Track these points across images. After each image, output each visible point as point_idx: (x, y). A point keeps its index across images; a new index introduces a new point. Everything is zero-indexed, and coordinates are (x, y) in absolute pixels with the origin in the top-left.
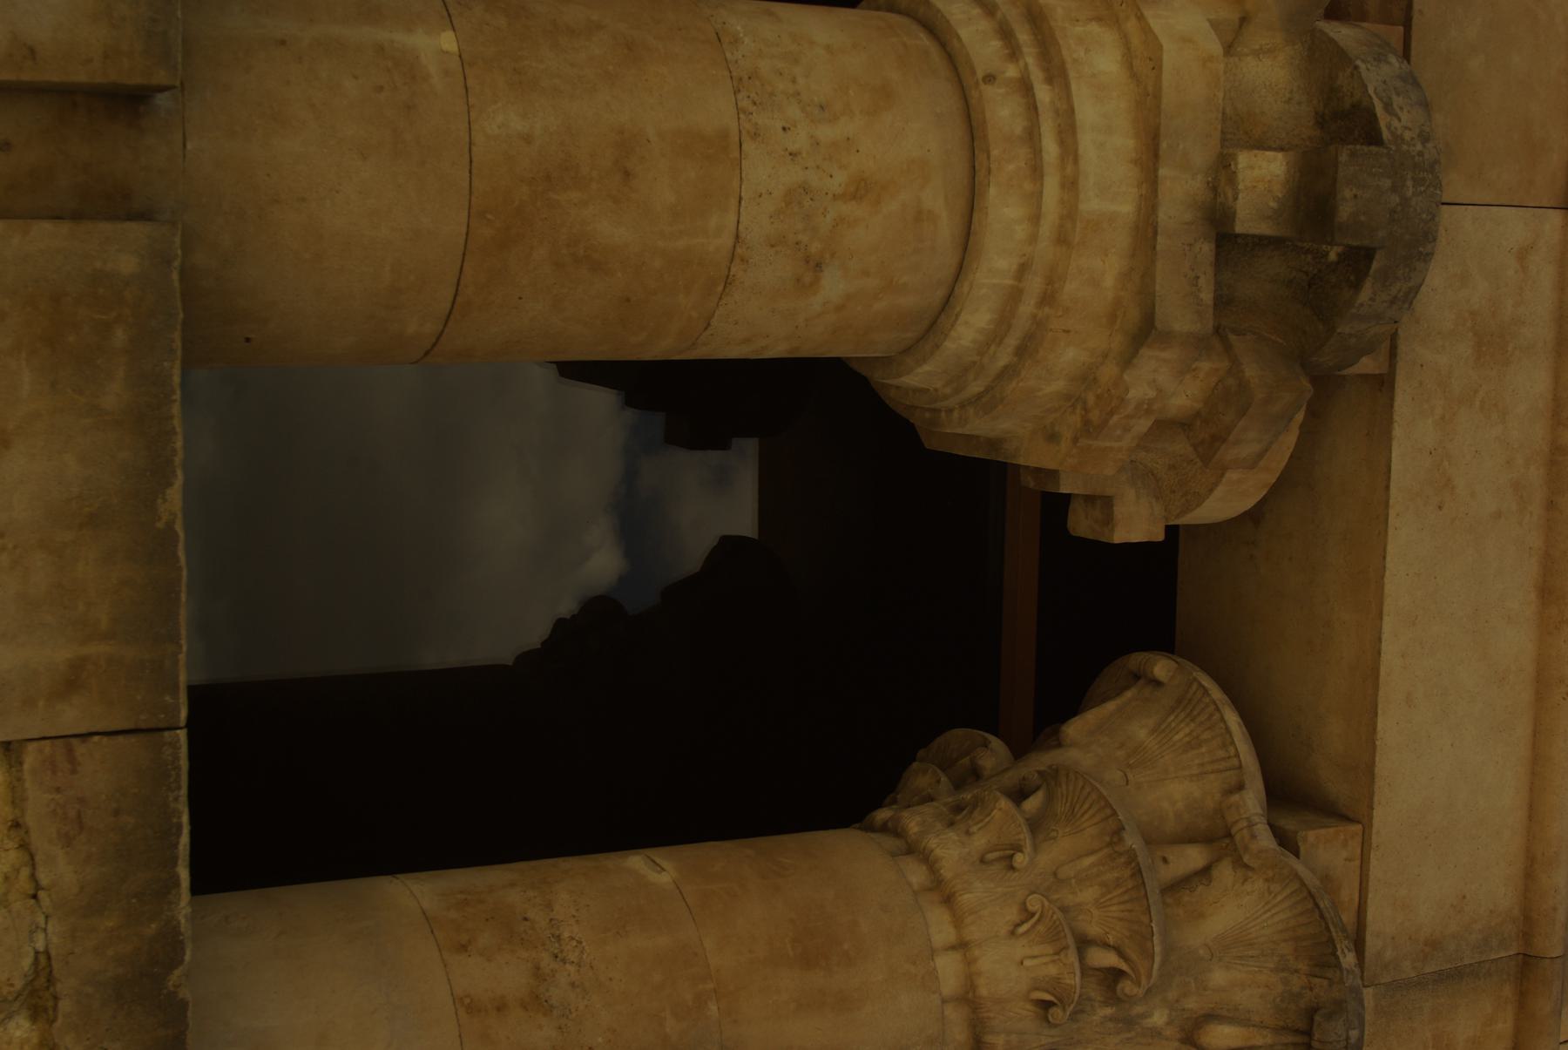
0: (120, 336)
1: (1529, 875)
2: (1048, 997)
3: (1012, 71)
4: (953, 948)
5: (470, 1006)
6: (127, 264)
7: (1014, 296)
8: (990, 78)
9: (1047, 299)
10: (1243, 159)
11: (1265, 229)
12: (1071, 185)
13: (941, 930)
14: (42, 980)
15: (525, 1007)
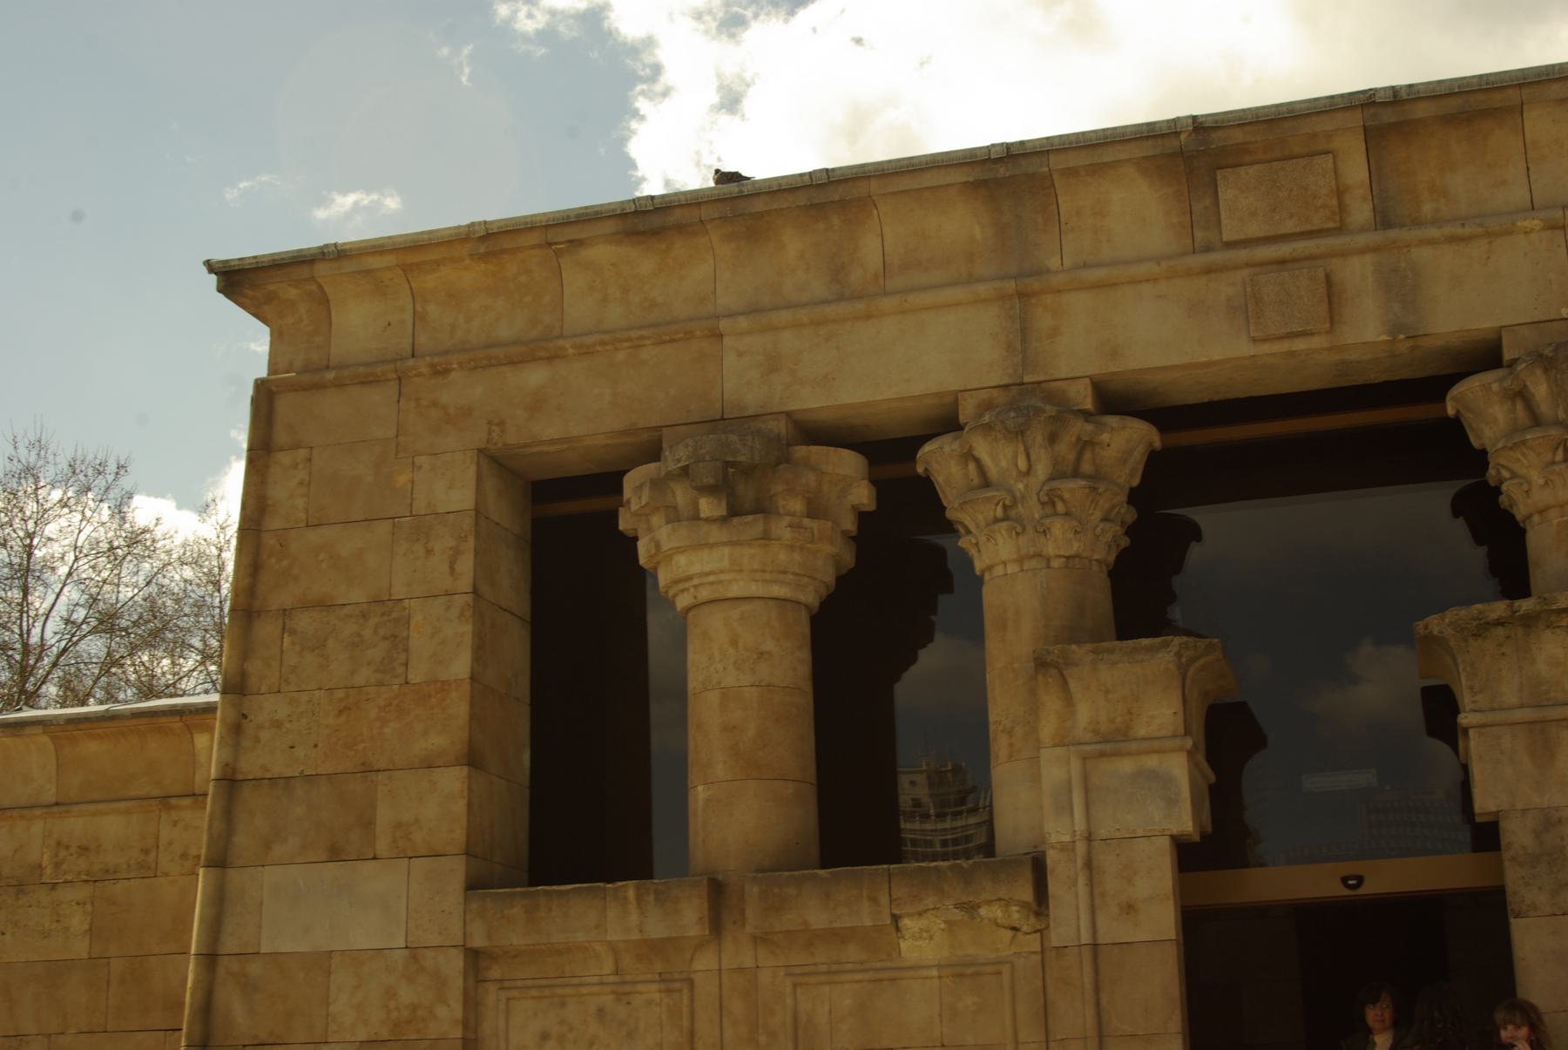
0: (776, 890)
1: (984, 301)
2: (1014, 533)
3: (692, 590)
4: (1005, 566)
5: (1010, 756)
6: (756, 889)
7: (765, 581)
8: (695, 597)
9: (764, 571)
10: (702, 515)
11: (724, 504)
12: (722, 572)
13: (999, 571)
14: (965, 906)
15: (1011, 737)
